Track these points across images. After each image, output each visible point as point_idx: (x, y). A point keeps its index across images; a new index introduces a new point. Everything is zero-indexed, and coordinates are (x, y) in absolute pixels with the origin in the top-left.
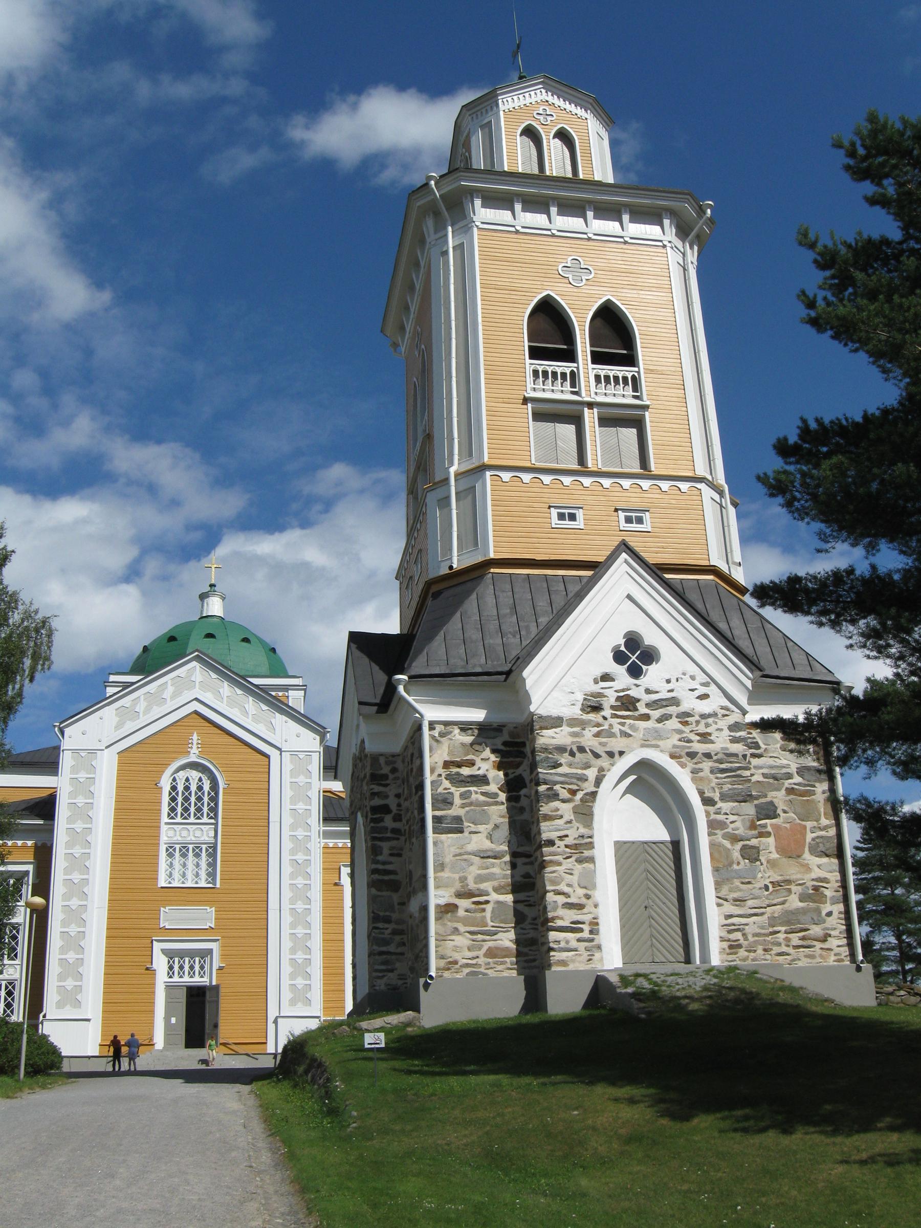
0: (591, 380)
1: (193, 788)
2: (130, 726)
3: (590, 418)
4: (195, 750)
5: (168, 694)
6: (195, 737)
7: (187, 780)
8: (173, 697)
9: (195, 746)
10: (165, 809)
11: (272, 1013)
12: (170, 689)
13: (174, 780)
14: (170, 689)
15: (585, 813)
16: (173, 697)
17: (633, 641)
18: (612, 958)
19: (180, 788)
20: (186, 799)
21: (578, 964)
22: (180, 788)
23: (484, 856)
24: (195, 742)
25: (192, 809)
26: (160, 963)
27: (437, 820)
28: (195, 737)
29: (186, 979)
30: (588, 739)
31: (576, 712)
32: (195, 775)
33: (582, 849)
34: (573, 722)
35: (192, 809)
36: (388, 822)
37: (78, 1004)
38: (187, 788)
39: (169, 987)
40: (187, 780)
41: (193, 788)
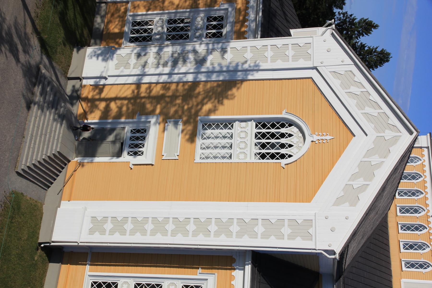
1: (283, 141)
2: (335, 83)
4: (315, 138)
5: (368, 110)
6: (328, 137)
7: (290, 135)
8: (366, 114)
9: (319, 138)
12: (375, 112)
13: (290, 125)
14: (375, 112)
16: (366, 114)
19: (283, 130)
20: (273, 136)
22: (283, 130)
24: (323, 138)
25: (264, 141)
28: (328, 137)
35: (264, 141)
38: (283, 135)
40: (290, 135)
41: (283, 141)
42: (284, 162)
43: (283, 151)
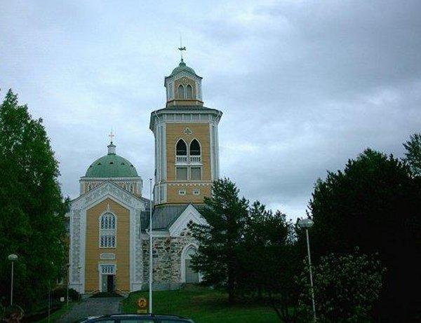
0: (188, 161)
3: (189, 170)
10: (100, 226)
11: (131, 282)
15: (180, 255)
17: (191, 222)
18: (183, 280)
21: (177, 281)
23: (161, 262)
26: (100, 269)
27: (153, 256)
29: (107, 273)
30: (181, 241)
31: (179, 236)
32: (108, 216)
33: (179, 261)
34: (179, 238)
36: (146, 253)
37: (79, 280)
39: (103, 276)
42: (116, 219)
43: (112, 219)
